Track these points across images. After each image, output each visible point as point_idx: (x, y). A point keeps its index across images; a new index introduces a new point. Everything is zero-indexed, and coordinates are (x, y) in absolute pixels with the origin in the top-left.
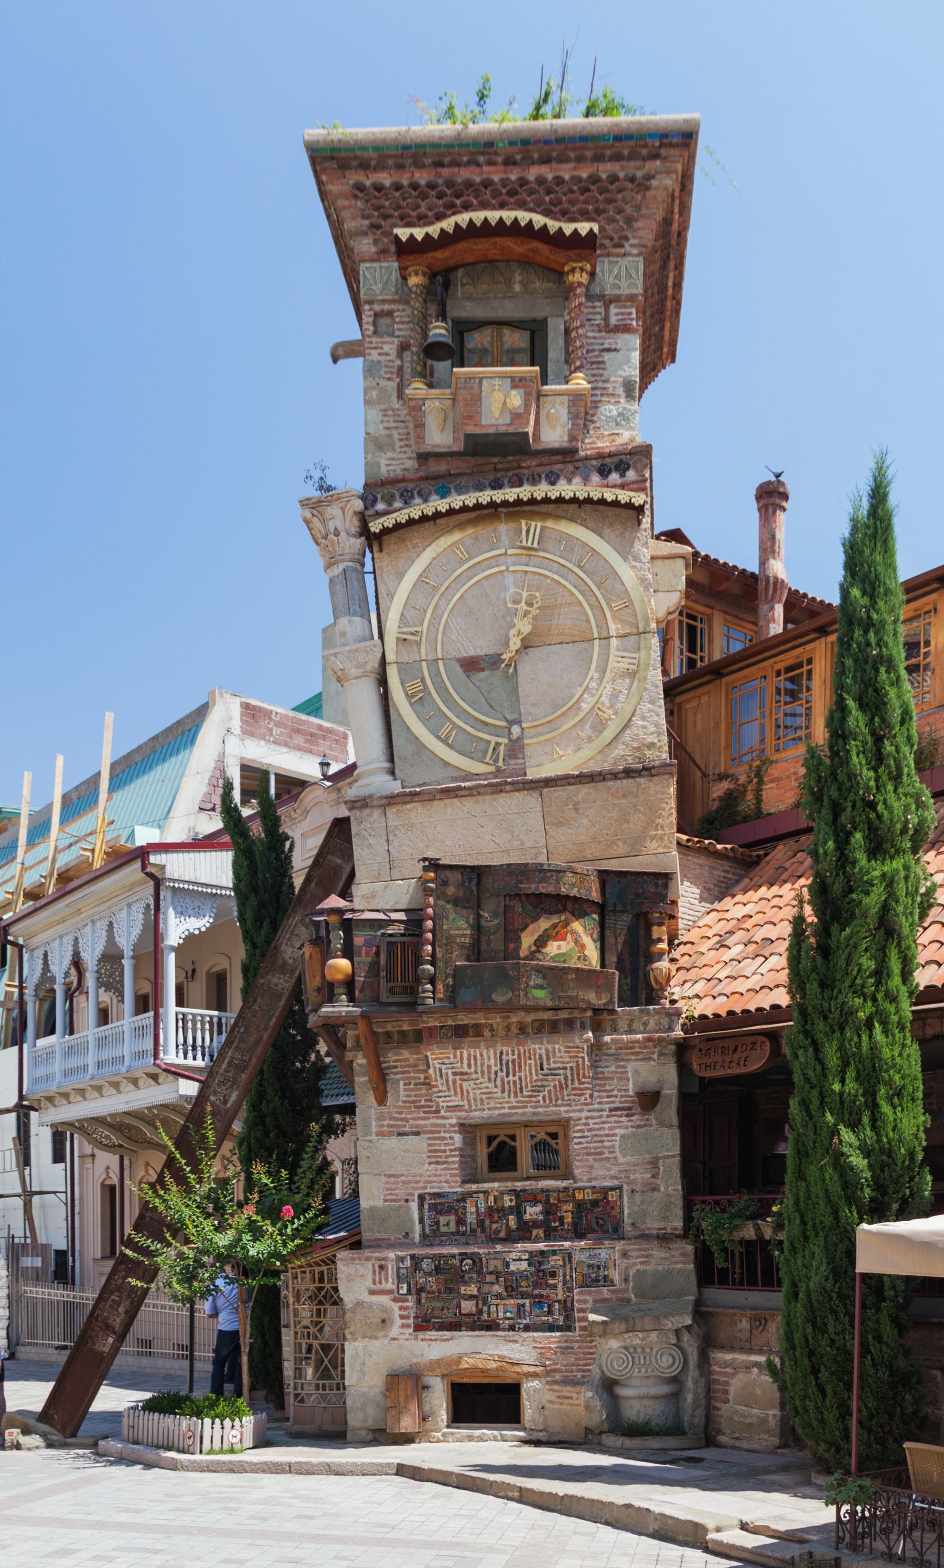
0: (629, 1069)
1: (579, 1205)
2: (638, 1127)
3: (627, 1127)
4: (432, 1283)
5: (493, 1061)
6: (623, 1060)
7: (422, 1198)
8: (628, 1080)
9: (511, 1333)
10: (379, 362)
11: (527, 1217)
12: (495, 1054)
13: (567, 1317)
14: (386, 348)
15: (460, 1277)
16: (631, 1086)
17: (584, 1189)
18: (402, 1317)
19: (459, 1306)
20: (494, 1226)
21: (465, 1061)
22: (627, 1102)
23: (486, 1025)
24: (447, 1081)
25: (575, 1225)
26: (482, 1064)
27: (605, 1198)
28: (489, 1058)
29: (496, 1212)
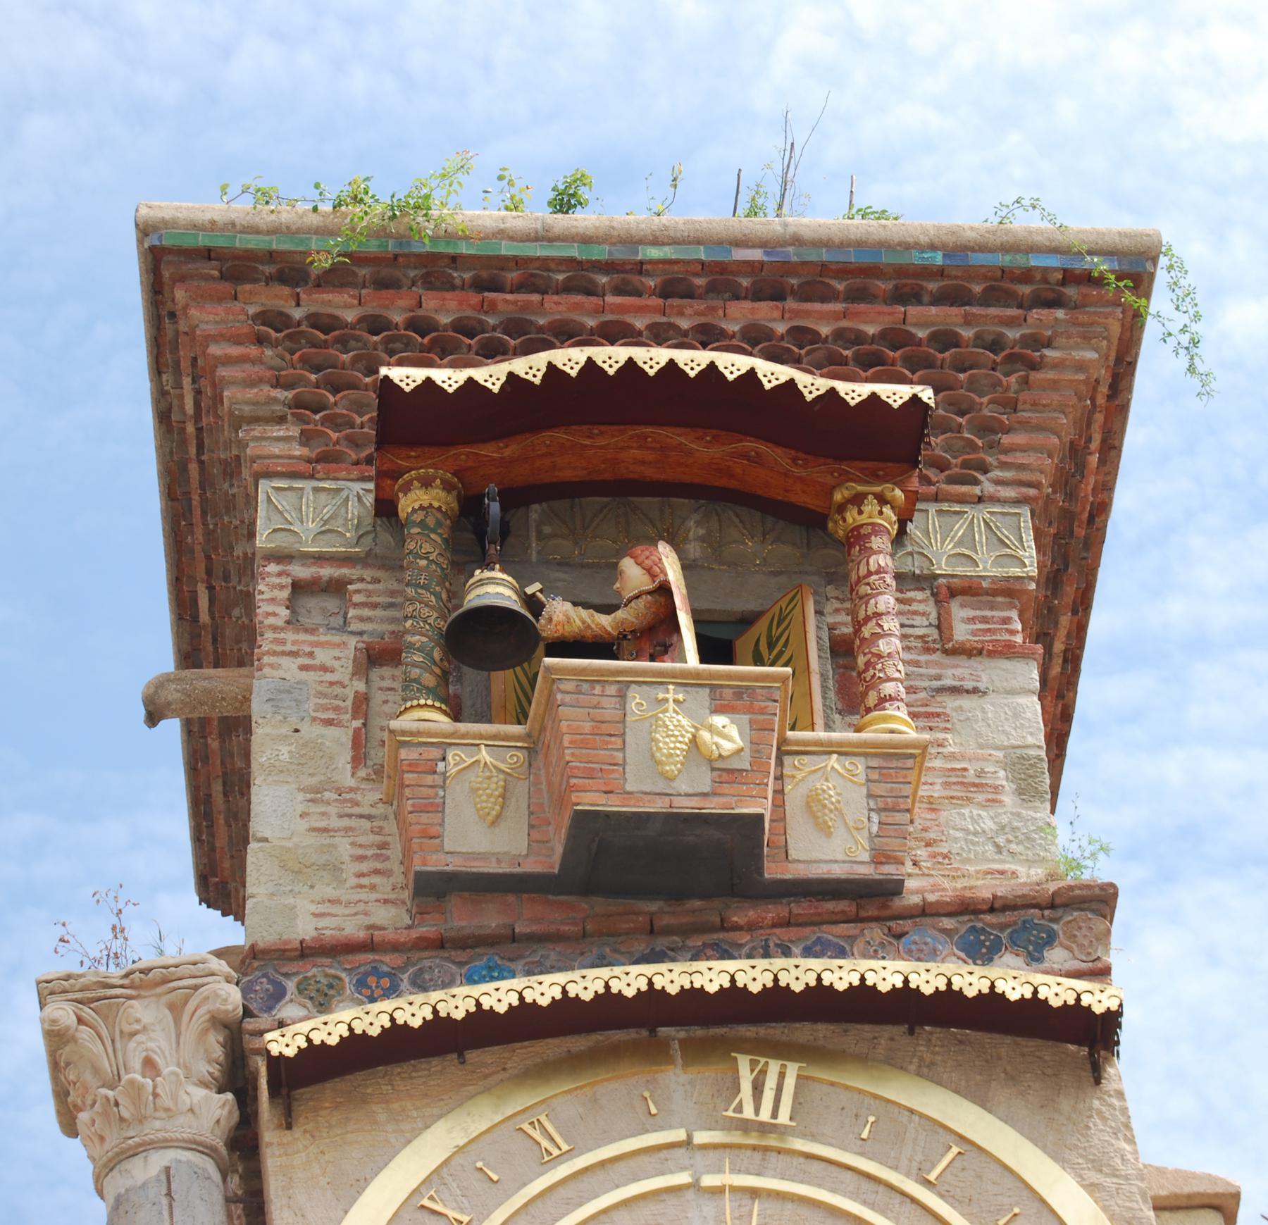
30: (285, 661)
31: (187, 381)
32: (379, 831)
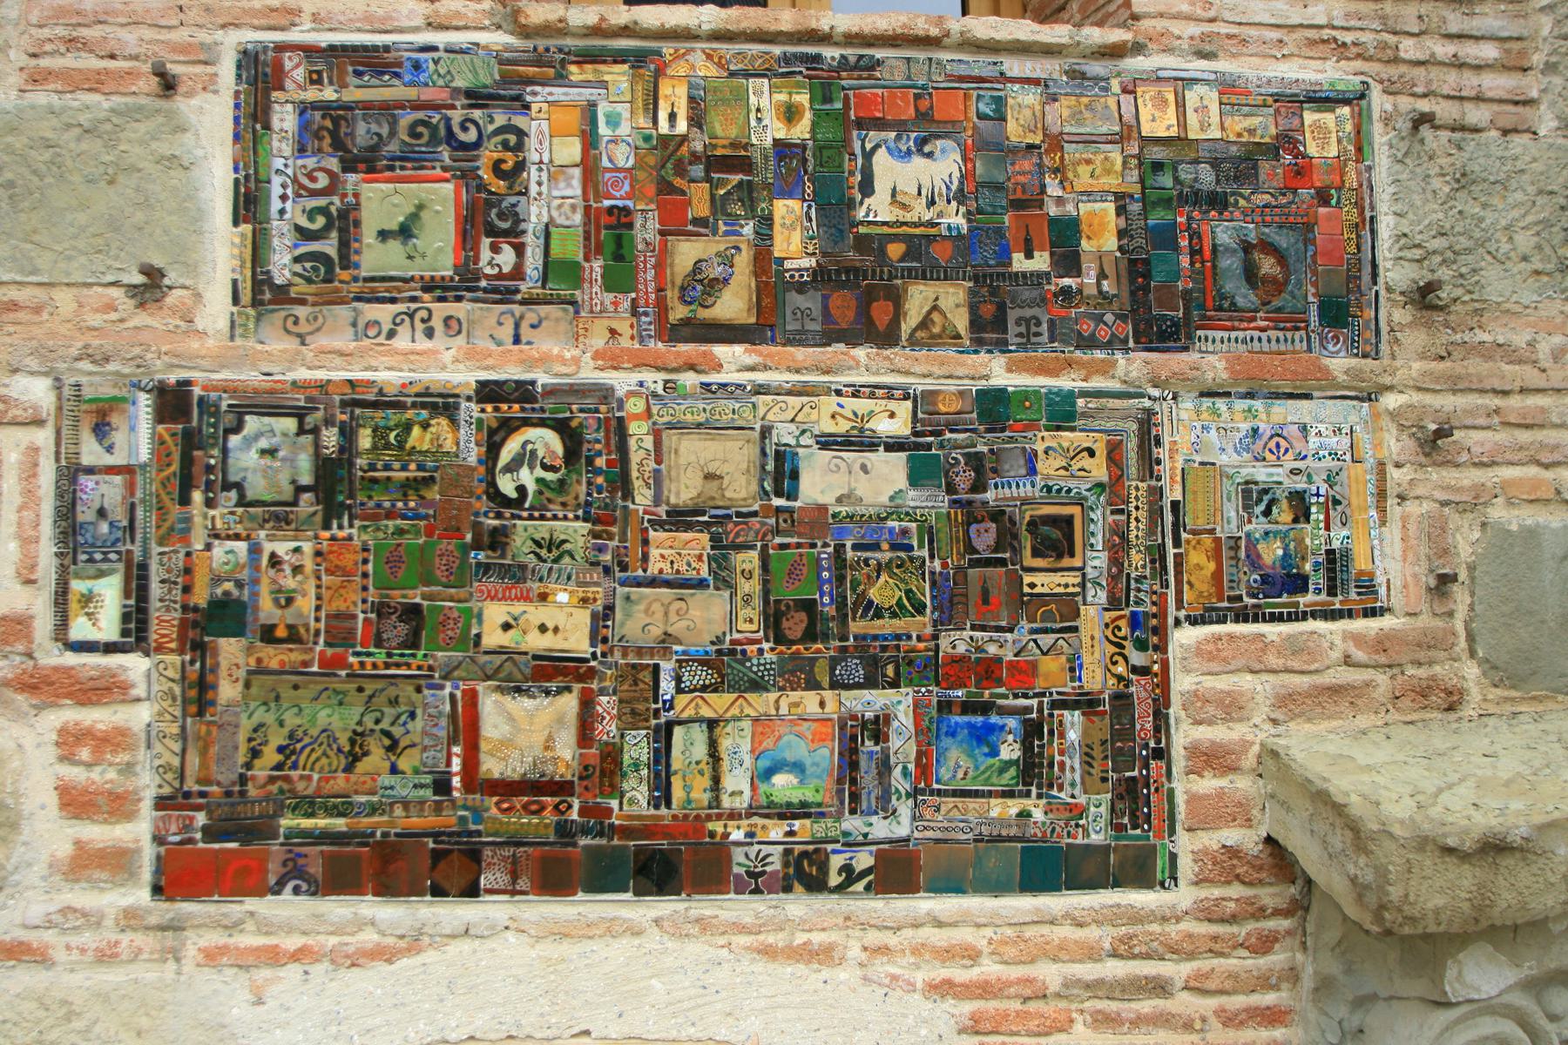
4: (296, 574)
9: (798, 905)
11: (877, 208)
18: (76, 803)
19: (466, 728)
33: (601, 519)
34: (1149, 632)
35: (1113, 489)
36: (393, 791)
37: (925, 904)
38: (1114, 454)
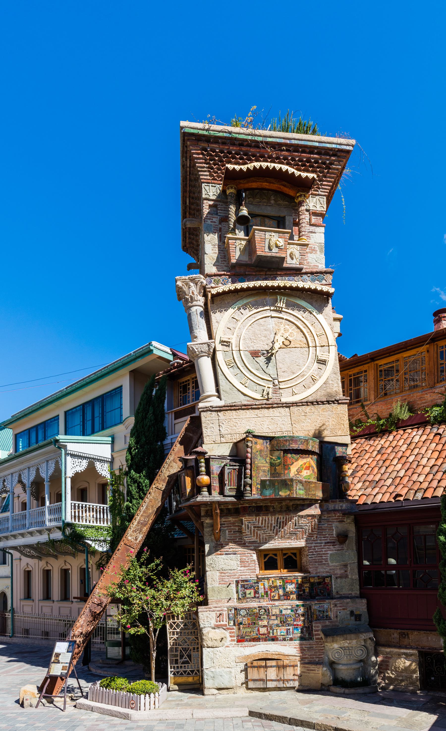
0: (333, 525)
1: (312, 584)
2: (338, 550)
3: (333, 550)
4: (246, 621)
5: (273, 522)
6: (331, 522)
7: (237, 582)
8: (333, 530)
9: (284, 642)
10: (211, 225)
11: (288, 590)
12: (275, 518)
13: (309, 634)
14: (214, 220)
15: (258, 617)
16: (334, 533)
17: (314, 577)
18: (231, 636)
19: (259, 630)
20: (272, 594)
21: (260, 522)
22: (333, 539)
23: (270, 506)
24: (251, 530)
25: (310, 593)
26: (268, 523)
27: (324, 581)
28: (272, 521)
29: (273, 588)
30: (208, 220)
31: (188, 160)
32: (224, 253)
33: (268, 615)
34: (311, 622)
35: (308, 611)
36: (254, 635)
37: (293, 642)
38: (307, 608)
